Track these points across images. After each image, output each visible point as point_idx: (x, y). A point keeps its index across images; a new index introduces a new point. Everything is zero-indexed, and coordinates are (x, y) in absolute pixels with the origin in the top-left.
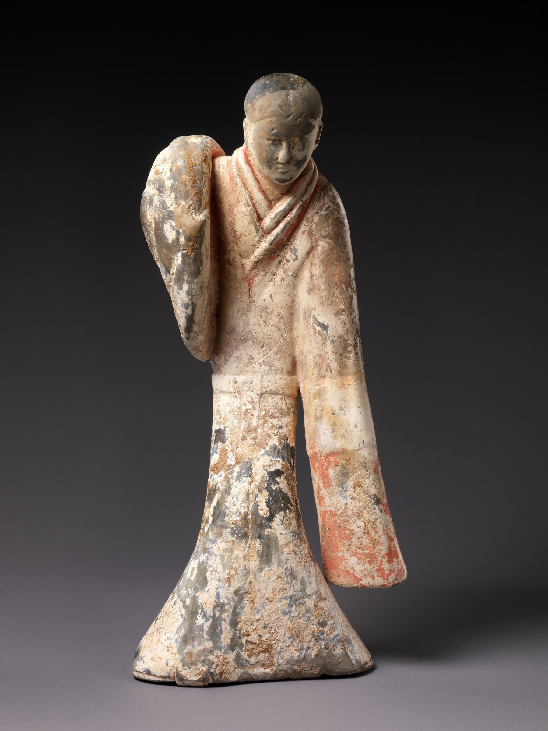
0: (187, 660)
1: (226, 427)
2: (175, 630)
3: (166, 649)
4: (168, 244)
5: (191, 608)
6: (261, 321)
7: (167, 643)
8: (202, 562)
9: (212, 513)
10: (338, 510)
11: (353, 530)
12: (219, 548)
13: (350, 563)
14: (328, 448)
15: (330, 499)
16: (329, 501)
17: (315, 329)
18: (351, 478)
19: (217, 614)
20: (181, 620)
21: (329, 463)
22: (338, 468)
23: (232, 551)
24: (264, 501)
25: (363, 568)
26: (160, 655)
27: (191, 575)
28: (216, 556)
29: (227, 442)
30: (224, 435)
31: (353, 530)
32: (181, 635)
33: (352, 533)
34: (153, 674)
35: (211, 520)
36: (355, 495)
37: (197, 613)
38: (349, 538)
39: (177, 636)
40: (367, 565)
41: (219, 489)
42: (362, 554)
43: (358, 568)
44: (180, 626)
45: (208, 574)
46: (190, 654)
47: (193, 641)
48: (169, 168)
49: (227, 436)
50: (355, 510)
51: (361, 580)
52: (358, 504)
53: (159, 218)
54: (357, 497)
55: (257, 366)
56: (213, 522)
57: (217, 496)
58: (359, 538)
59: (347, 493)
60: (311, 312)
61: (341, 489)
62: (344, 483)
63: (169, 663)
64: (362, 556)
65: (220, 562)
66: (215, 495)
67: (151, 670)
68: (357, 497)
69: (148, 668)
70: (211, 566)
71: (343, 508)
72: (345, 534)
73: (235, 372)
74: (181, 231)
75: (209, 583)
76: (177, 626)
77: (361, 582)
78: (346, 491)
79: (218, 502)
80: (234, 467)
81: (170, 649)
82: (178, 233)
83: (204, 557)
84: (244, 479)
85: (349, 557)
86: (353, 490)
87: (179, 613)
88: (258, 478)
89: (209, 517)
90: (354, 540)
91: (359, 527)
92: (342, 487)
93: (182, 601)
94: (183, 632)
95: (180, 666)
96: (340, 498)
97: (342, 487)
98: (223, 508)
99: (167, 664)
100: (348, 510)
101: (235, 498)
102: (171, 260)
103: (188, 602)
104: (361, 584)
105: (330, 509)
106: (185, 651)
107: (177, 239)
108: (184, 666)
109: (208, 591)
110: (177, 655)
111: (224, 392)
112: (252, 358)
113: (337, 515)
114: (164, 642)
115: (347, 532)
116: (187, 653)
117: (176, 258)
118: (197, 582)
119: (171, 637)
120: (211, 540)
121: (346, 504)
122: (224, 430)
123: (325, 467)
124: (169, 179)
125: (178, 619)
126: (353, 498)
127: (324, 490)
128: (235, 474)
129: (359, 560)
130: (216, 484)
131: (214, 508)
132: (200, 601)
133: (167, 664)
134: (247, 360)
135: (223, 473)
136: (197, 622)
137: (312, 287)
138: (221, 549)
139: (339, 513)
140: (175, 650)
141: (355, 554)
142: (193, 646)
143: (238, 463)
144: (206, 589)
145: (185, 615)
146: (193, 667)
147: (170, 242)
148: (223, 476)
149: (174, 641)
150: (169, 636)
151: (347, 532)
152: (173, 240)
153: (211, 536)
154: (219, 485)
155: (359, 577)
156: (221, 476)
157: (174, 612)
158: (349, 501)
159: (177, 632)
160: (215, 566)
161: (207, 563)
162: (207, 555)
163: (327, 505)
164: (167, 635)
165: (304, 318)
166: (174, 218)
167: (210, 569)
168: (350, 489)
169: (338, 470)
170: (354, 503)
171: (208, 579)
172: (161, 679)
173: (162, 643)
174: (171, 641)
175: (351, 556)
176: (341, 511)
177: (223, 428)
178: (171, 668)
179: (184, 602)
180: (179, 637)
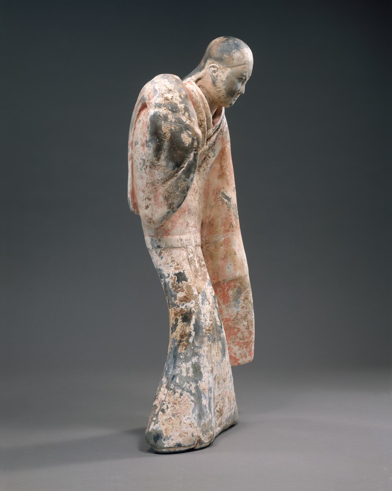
0: (204, 430)
1: (184, 271)
2: (191, 411)
3: (190, 426)
4: (184, 147)
5: (197, 394)
6: (193, 198)
7: (188, 422)
8: (195, 362)
9: (193, 329)
10: (232, 317)
11: (239, 328)
12: (204, 351)
13: (233, 351)
14: (231, 277)
15: (227, 310)
16: (226, 312)
17: (223, 201)
18: (243, 295)
19: (210, 394)
20: (193, 404)
21: (230, 287)
22: (235, 290)
23: (211, 352)
24: (217, 315)
25: (241, 352)
26: (185, 431)
27: (188, 373)
28: (204, 356)
29: (189, 280)
30: (185, 276)
31: (239, 328)
32: (197, 414)
33: (239, 330)
34: (183, 445)
35: (193, 333)
36: (244, 305)
37: (201, 397)
38: (236, 334)
39: (194, 415)
40: (244, 349)
41: (194, 312)
42: (243, 343)
43: (238, 353)
44: (194, 408)
45: (202, 369)
46: (204, 425)
47: (204, 416)
48: (178, 95)
49: (187, 276)
50: (243, 315)
51: (238, 360)
52: (245, 310)
53: (175, 130)
54: (245, 306)
55: (190, 228)
56: (196, 335)
57: (194, 317)
58: (242, 333)
59: (240, 304)
60: (220, 190)
61: (236, 303)
62: (238, 298)
63: (194, 435)
64: (242, 344)
65: (207, 360)
66: (192, 317)
67: (182, 443)
68: (245, 306)
69: (178, 442)
70: (202, 364)
71: (235, 315)
72: (234, 331)
73: (179, 233)
74: (195, 138)
75: (204, 375)
76: (192, 409)
77: (238, 362)
78: (239, 303)
79: (196, 320)
80: (198, 296)
81: (192, 425)
82: (193, 139)
83: (196, 359)
84: (206, 302)
85: (233, 347)
86: (243, 301)
87: (190, 400)
88: (211, 301)
89: (191, 332)
90: (239, 334)
91: (244, 326)
92: (237, 301)
93: (187, 391)
94: (197, 412)
95: (201, 435)
96: (235, 308)
97: (237, 301)
98: (201, 324)
99: (193, 436)
100: (239, 316)
101: (205, 316)
102: (184, 158)
103: (193, 392)
104: (238, 363)
105: (226, 317)
106: (202, 424)
107: (192, 143)
108: (203, 434)
109: (204, 381)
110: (198, 428)
111: (176, 248)
112: (188, 223)
113: (230, 320)
114: (185, 422)
115: (236, 330)
116: (203, 425)
117: (189, 156)
118: (195, 376)
119: (190, 416)
120: (197, 347)
121: (238, 312)
122: (184, 272)
123: (226, 290)
124: (181, 103)
125: (191, 404)
126: (243, 307)
127: (223, 305)
128: (200, 301)
129: (240, 347)
130: (191, 309)
131: (194, 325)
132: (201, 388)
133: (193, 436)
134: (186, 225)
135: (193, 301)
136: (203, 403)
137: (221, 174)
138: (206, 351)
139: (232, 319)
140: (196, 425)
141: (238, 344)
142: (205, 419)
143: (199, 293)
144: (203, 379)
145: (195, 400)
146: (207, 433)
147: (187, 145)
148: (194, 303)
149: (193, 419)
150: (188, 417)
151: (236, 330)
152: (189, 144)
153: (197, 344)
154: (193, 309)
155: (238, 358)
156: (192, 303)
157: (184, 400)
158: (240, 309)
159: (193, 413)
160: (204, 363)
161: (199, 363)
162: (197, 357)
163: (224, 315)
164: (186, 417)
165: (213, 194)
166: (190, 129)
167: (202, 366)
168: (242, 301)
169: (235, 291)
170: (243, 311)
171: (203, 372)
172: (187, 448)
173: (185, 423)
174: (191, 420)
175: (235, 346)
176: (233, 317)
177: (182, 272)
178: (196, 438)
179: (191, 392)
180: (195, 415)
